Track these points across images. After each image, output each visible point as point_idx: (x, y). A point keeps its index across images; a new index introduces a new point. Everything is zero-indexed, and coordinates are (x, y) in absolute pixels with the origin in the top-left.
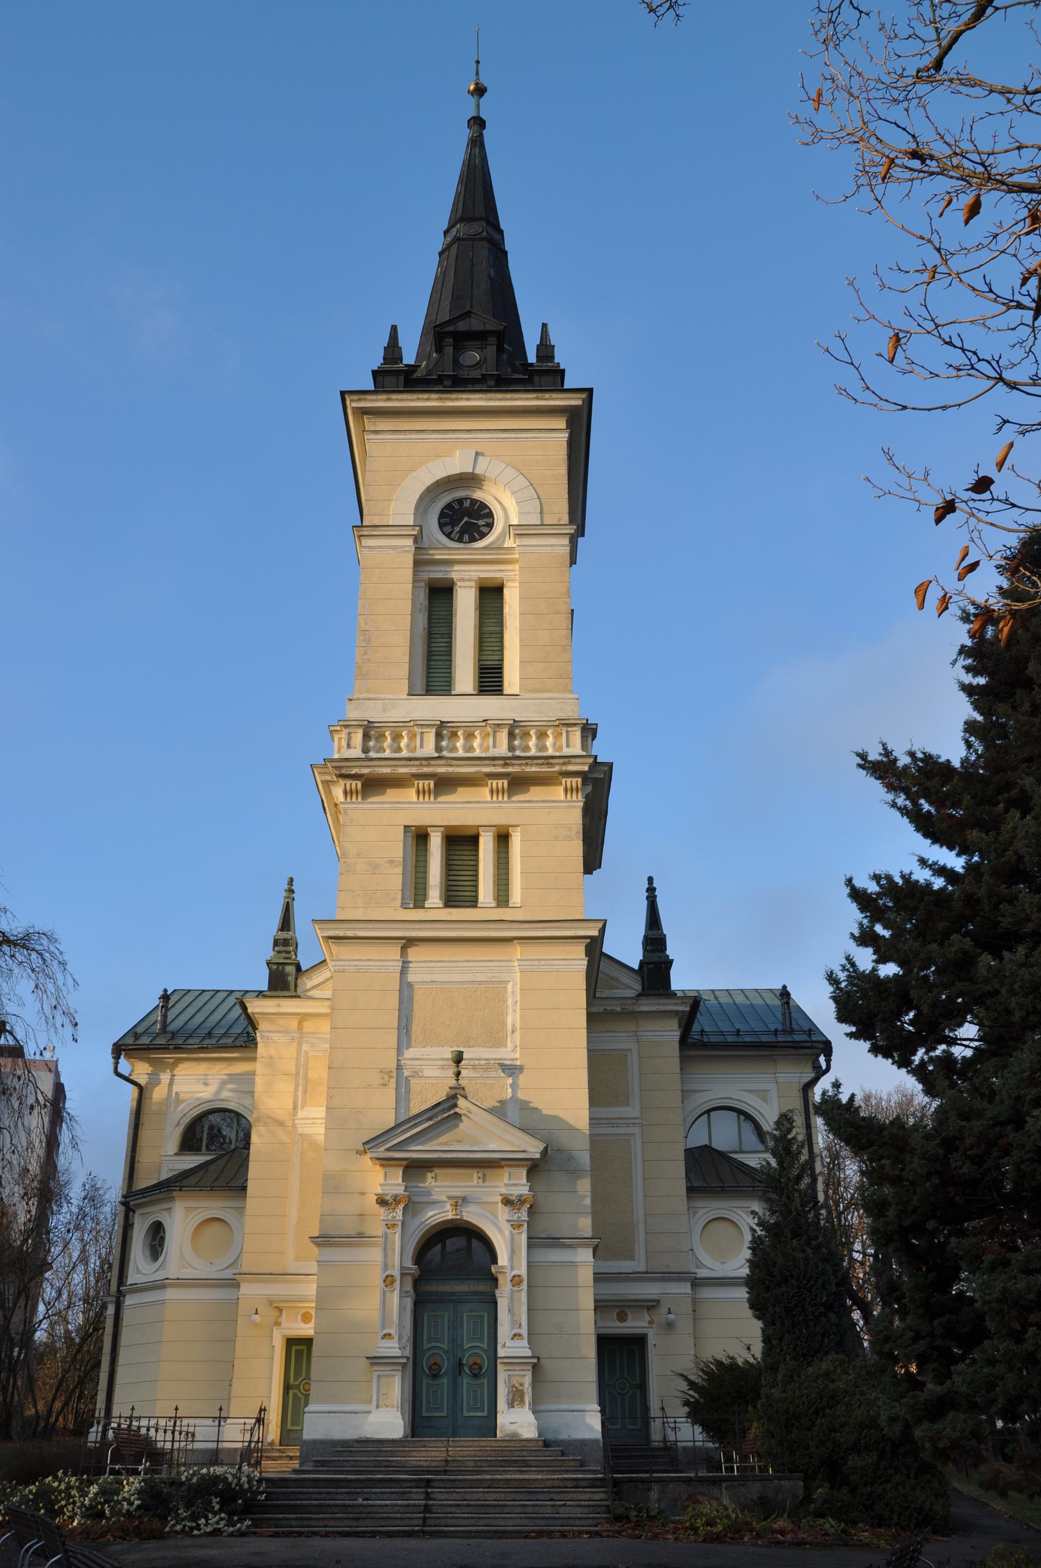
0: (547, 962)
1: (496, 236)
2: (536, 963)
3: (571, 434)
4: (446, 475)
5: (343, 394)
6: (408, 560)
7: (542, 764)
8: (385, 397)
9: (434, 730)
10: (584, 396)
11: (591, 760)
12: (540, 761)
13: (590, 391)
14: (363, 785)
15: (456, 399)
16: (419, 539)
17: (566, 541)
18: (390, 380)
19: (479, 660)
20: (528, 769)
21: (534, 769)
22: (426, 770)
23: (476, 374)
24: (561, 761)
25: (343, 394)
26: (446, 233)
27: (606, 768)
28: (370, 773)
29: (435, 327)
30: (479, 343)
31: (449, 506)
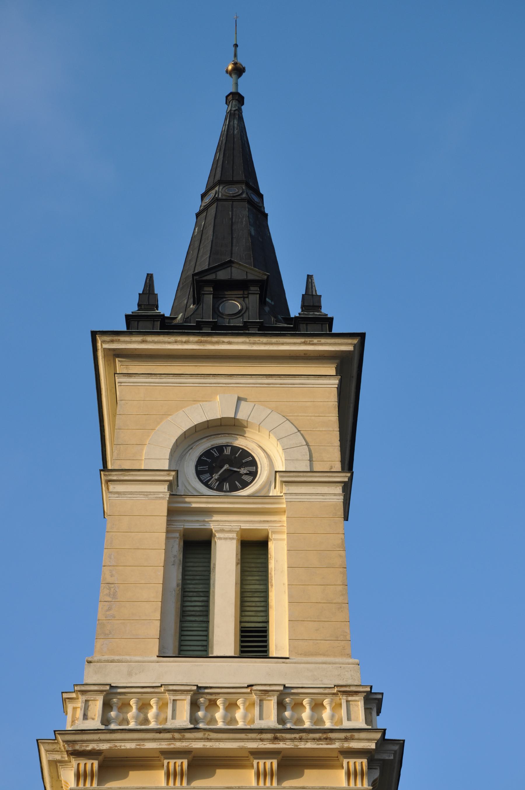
1: (256, 199)
3: (341, 381)
4: (204, 419)
5: (94, 334)
6: (162, 507)
7: (320, 739)
8: (139, 338)
9: (188, 698)
10: (355, 341)
11: (378, 736)
12: (317, 736)
13: (362, 336)
14: (100, 767)
15: (218, 343)
16: (175, 487)
17: (339, 490)
18: (144, 326)
19: (241, 622)
20: (302, 745)
21: (310, 745)
22: (179, 745)
23: (238, 322)
24: (342, 735)
25: (94, 334)
26: (203, 196)
27: (396, 748)
28: (110, 749)
29: (193, 275)
30: (241, 292)
31: (207, 453)
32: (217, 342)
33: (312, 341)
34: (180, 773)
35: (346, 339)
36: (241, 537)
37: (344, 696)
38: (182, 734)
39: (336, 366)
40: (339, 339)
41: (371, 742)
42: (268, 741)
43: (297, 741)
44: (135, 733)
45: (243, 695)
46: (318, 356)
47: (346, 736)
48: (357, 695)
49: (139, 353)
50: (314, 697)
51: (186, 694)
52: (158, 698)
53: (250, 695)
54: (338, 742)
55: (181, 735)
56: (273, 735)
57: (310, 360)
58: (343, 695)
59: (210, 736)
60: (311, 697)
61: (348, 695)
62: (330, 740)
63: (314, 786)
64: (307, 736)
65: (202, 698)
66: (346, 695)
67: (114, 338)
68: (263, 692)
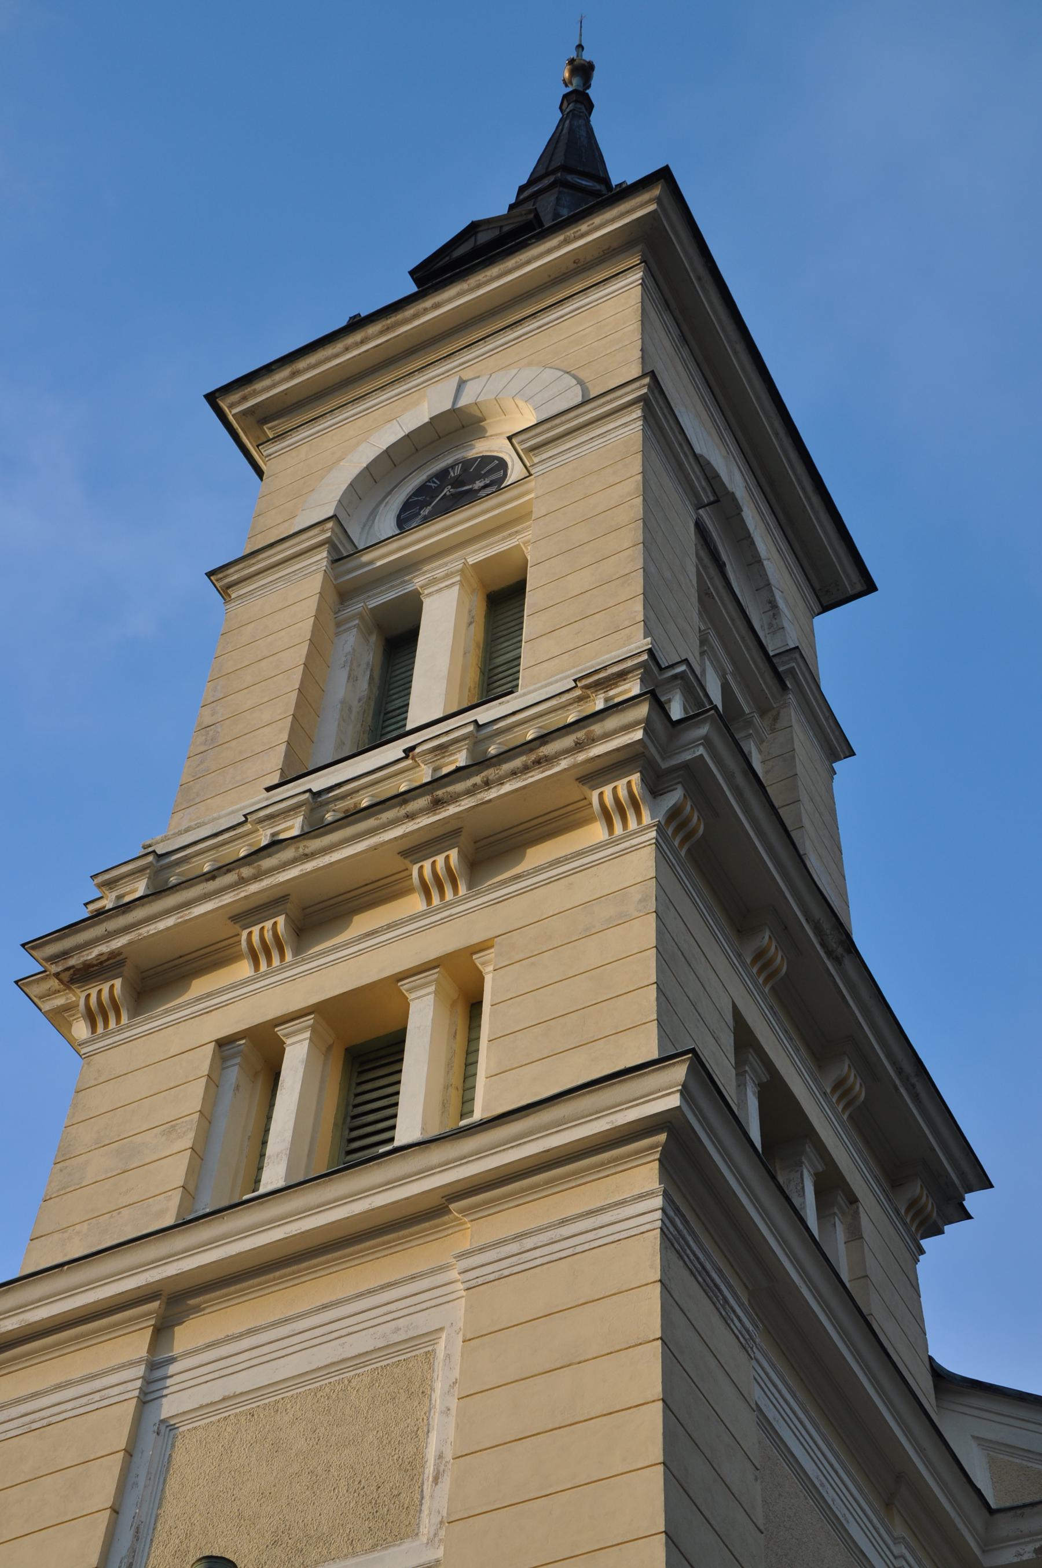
0: (543, 1238)
2: (513, 1248)
5: (212, 398)
7: (526, 769)
10: (656, 192)
12: (517, 763)
15: (416, 316)
24: (568, 741)
25: (212, 398)
32: (414, 315)
33: (577, 231)
34: (274, 943)
35: (637, 197)
36: (483, 584)
37: (599, 693)
38: (256, 864)
39: (640, 257)
40: (624, 203)
41: (632, 731)
42: (424, 815)
43: (481, 792)
44: (168, 895)
45: (403, 775)
46: (602, 254)
47: (576, 740)
48: (625, 680)
49: (295, 401)
50: (543, 721)
51: (293, 815)
52: (248, 845)
53: (417, 769)
54: (565, 758)
55: (253, 868)
56: (428, 797)
57: (590, 269)
58: (596, 691)
59: (308, 847)
60: (538, 723)
61: (607, 687)
62: (546, 761)
63: (537, 865)
64: (496, 772)
65: (328, 812)
66: (603, 689)
67: (246, 391)
68: (437, 753)
